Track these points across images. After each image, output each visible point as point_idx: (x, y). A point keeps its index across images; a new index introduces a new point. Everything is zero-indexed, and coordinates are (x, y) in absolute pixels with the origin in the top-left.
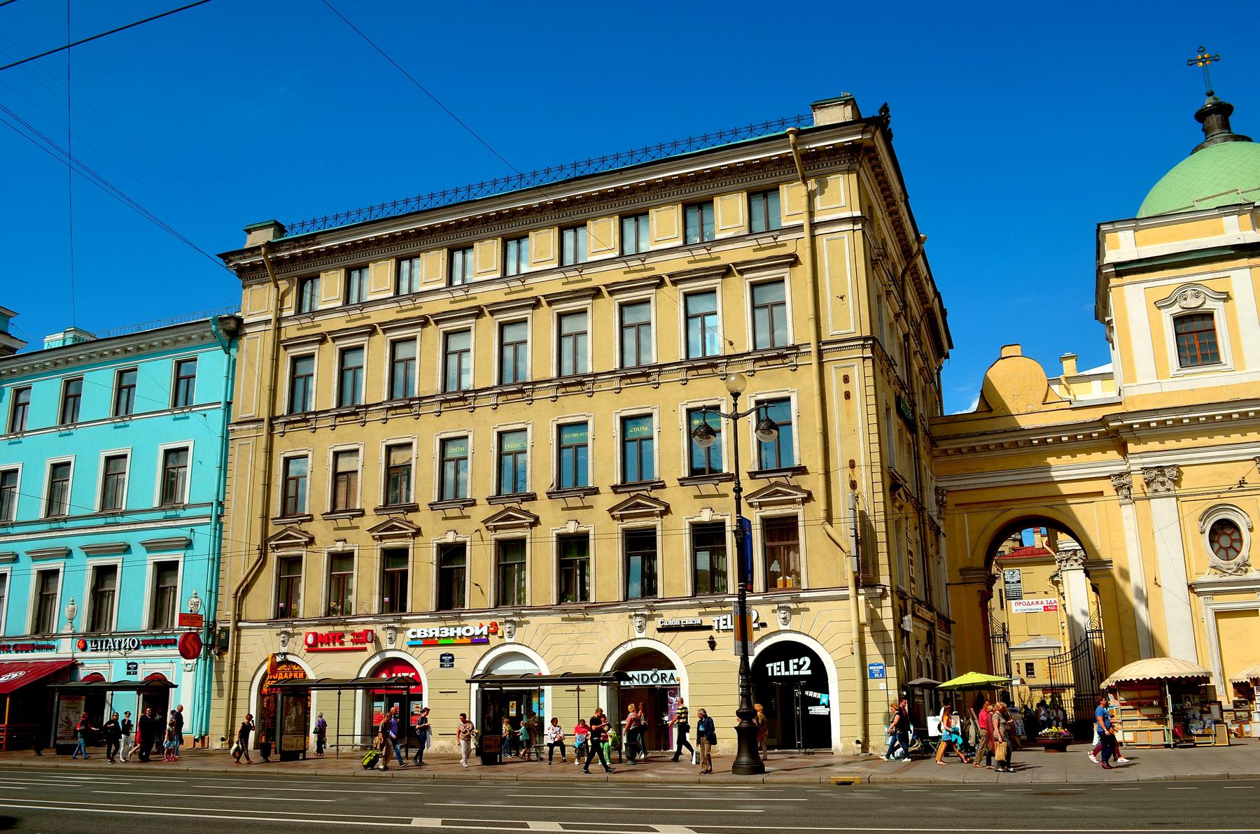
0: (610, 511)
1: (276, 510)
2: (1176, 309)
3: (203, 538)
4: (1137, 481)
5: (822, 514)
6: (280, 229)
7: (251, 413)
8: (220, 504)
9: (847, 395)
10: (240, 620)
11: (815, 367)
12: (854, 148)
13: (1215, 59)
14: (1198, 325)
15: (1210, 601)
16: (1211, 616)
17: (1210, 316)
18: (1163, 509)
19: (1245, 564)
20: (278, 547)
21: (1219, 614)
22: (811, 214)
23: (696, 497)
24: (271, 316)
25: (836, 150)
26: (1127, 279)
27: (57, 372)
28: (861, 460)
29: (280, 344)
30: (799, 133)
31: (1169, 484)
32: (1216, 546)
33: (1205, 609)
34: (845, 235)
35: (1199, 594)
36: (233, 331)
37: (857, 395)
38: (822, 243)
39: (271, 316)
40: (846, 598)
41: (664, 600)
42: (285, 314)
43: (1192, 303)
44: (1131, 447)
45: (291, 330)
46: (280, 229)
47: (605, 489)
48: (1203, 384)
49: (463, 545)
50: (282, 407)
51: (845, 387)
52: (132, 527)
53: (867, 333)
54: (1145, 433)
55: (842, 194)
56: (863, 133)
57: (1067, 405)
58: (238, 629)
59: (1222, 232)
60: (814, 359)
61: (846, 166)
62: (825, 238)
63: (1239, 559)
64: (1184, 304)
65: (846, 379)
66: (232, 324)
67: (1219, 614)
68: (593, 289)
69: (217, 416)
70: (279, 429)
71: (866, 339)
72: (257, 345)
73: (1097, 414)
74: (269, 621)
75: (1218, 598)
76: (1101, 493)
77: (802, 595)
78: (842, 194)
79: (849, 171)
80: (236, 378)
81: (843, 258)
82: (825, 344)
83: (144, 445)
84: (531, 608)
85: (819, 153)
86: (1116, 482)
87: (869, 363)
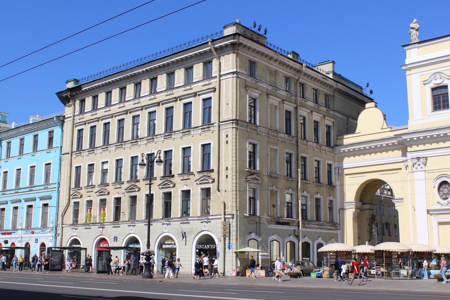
0: (159, 186)
1: (73, 186)
2: (432, 85)
3: (54, 195)
5: (216, 188)
6: (76, 81)
7: (67, 151)
8: (59, 183)
9: (227, 142)
10: (63, 224)
11: (217, 132)
12: (233, 44)
14: (443, 91)
15: (436, 218)
17: (446, 87)
18: (419, 175)
20: (73, 198)
21: (440, 224)
22: (220, 71)
23: (182, 180)
24: (71, 115)
25: (226, 46)
27: (17, 136)
28: (230, 168)
29: (74, 125)
30: (213, 41)
31: (422, 165)
32: (441, 193)
33: (435, 220)
34: (231, 79)
35: (431, 214)
36: (62, 120)
37: (230, 142)
38: (223, 83)
39: (71, 115)
40: (221, 218)
41: (172, 219)
42: (76, 114)
43: (439, 81)
44: (409, 149)
45: (77, 121)
46: (76, 81)
47: (158, 179)
49: (120, 198)
50: (75, 149)
51: (227, 139)
52: (38, 191)
53: (234, 118)
54: (412, 142)
55: (228, 63)
56: (234, 39)
57: (389, 129)
58: (63, 227)
60: (216, 129)
61: (232, 51)
62: (224, 81)
65: (227, 136)
66: (62, 118)
67: (440, 224)
68: (157, 103)
69: (58, 151)
70: (74, 156)
71: (233, 120)
72: (68, 124)
74: (112, 222)
76: (401, 169)
77: (210, 217)
78: (228, 63)
79: (234, 53)
80: (65, 137)
81: (229, 88)
82: (221, 122)
83: (40, 161)
84: (137, 221)
85: (221, 47)
86: (405, 164)
87: (234, 129)
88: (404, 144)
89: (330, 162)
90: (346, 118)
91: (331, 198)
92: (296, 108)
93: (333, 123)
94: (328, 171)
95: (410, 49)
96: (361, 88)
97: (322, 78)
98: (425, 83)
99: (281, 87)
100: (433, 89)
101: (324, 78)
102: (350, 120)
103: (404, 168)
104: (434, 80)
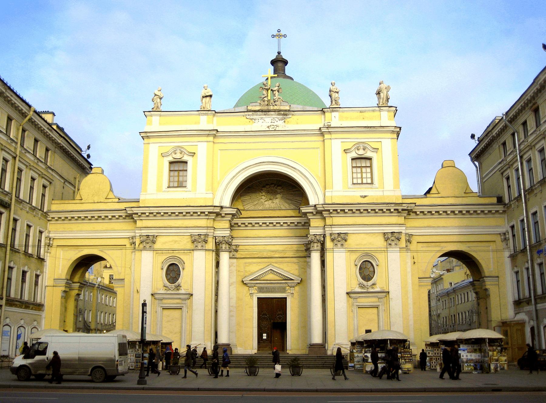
2: (171, 159)
4: (138, 242)
13: (285, 36)
16: (160, 309)
18: (147, 256)
19: (179, 286)
26: (151, 140)
43: (178, 156)
48: (177, 197)
59: (199, 123)
63: (176, 284)
64: (175, 156)
73: (122, 206)
75: (164, 301)
88: (133, 218)
89: (41, 229)
90: (63, 181)
91: (38, 273)
92: (15, 158)
93: (51, 183)
94: (39, 240)
95: (151, 116)
96: (81, 151)
97: (48, 128)
98: (163, 155)
99: (3, 128)
100: (171, 163)
101: (49, 130)
102: (66, 183)
103: (128, 246)
104: (173, 154)
